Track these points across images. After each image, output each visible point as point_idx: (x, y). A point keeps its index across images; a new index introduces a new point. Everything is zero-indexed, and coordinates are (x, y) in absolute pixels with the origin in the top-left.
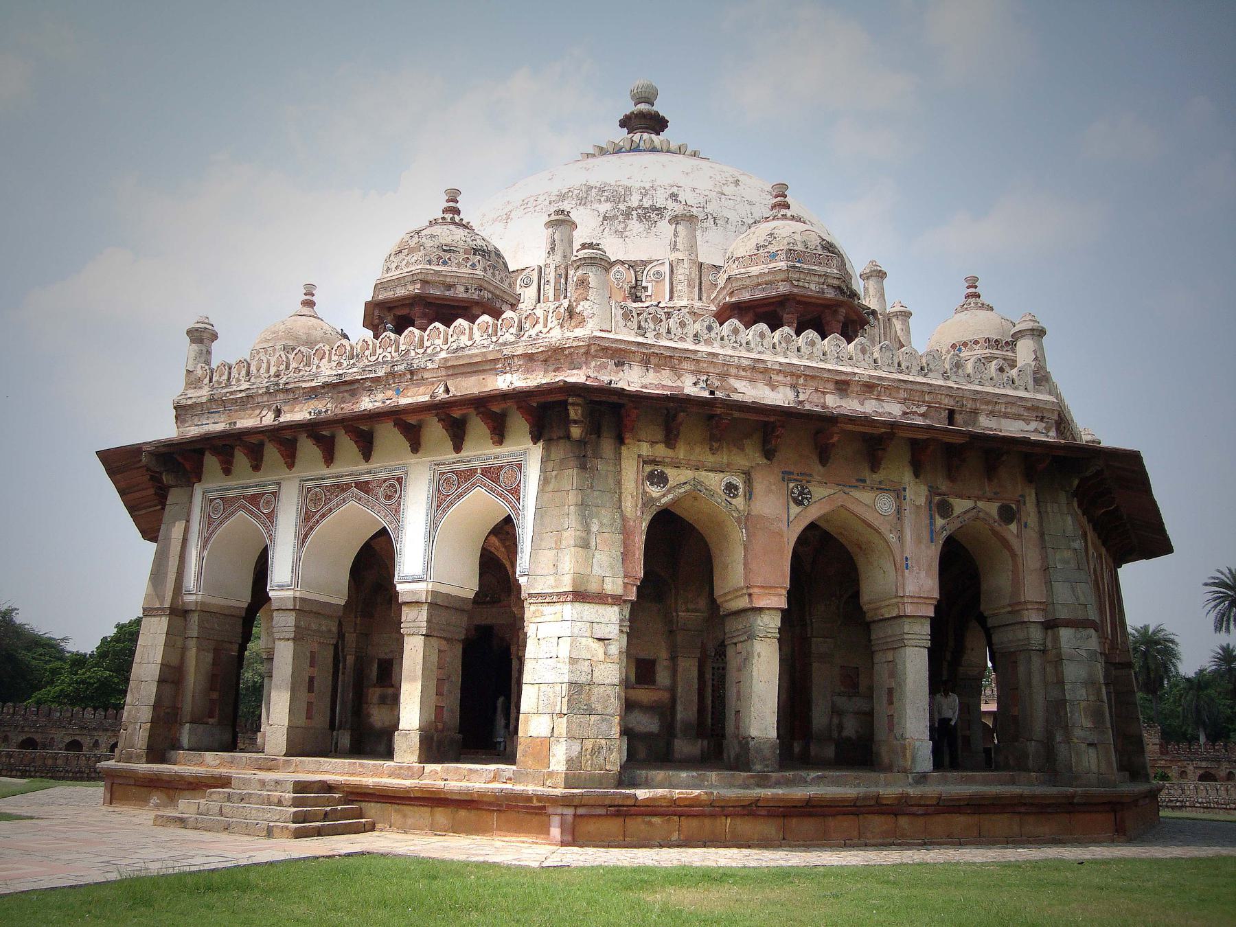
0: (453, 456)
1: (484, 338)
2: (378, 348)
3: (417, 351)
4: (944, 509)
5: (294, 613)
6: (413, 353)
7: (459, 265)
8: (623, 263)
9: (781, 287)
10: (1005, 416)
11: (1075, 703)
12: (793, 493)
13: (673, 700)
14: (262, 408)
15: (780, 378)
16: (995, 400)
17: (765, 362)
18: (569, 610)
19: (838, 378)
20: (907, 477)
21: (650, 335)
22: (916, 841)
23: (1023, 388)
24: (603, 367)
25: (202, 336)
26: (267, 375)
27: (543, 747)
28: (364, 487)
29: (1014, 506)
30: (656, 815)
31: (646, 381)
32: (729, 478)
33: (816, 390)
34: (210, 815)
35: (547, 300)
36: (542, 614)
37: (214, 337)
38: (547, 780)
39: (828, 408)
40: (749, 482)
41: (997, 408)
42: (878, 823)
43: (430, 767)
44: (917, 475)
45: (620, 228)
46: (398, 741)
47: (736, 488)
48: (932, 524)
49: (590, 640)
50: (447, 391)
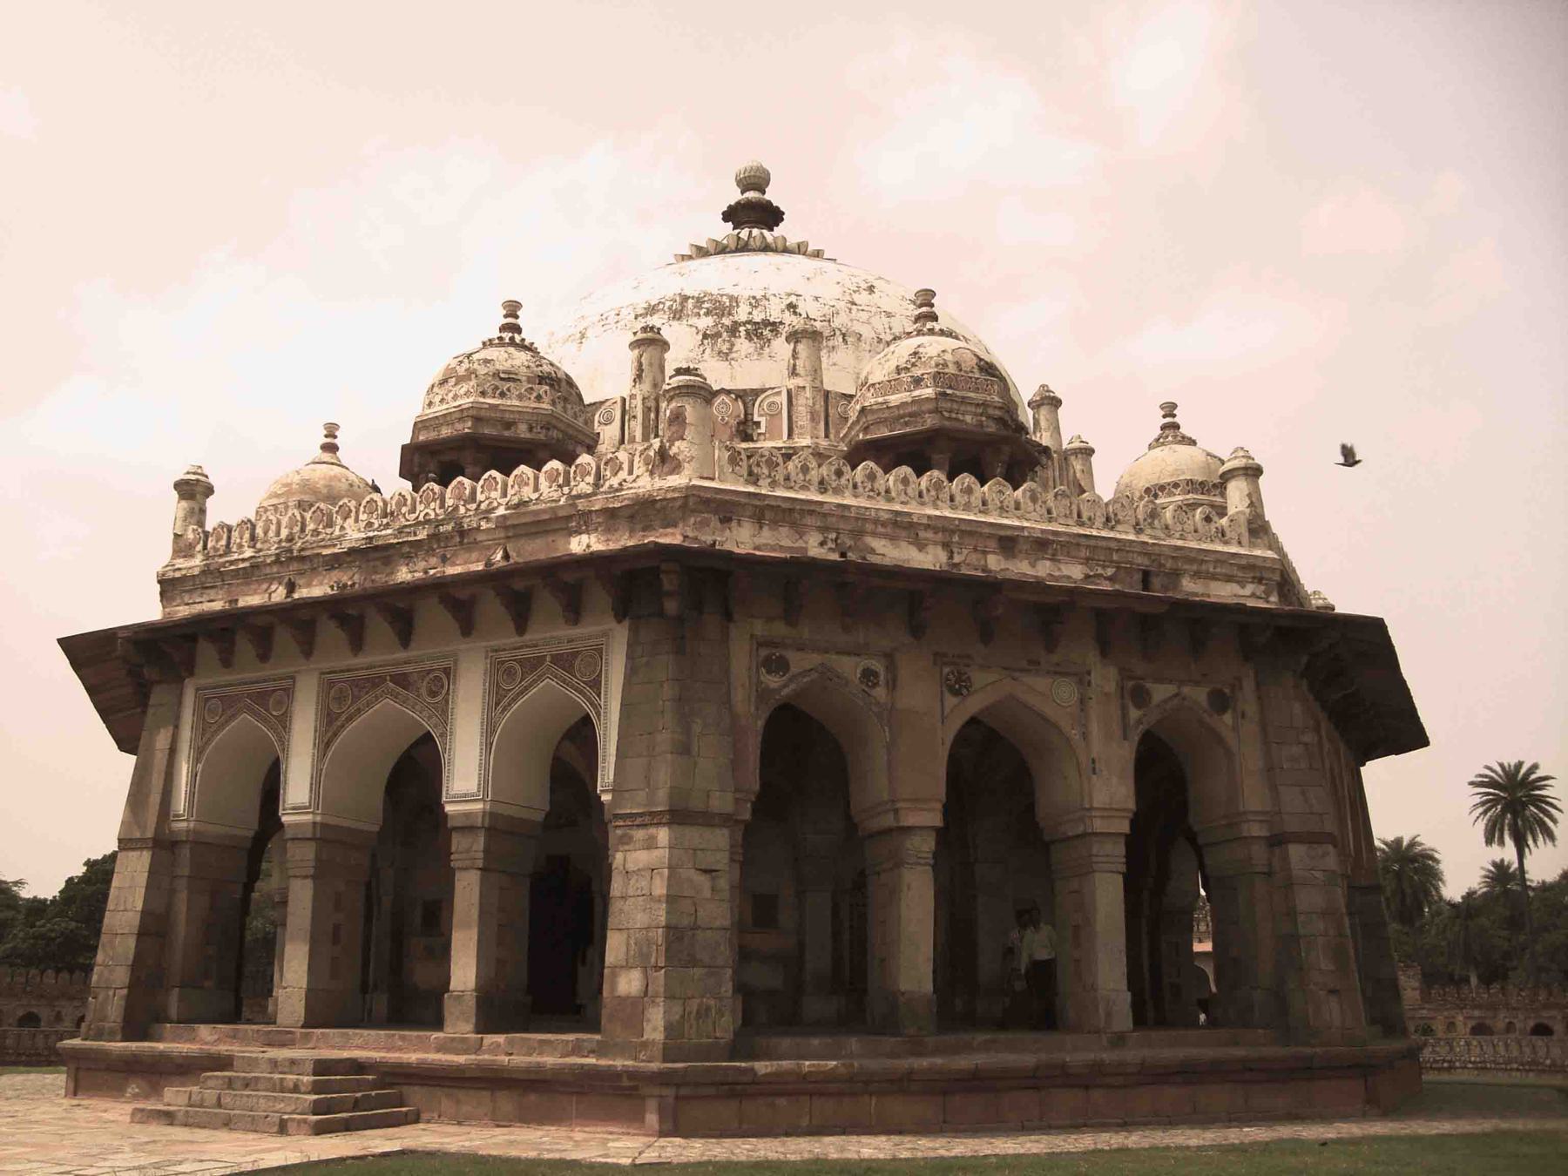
0: (515, 640)
1: (552, 489)
2: (418, 503)
3: (468, 506)
4: (1140, 696)
5: (313, 844)
6: (462, 510)
7: (520, 397)
8: (728, 392)
9: (929, 420)
10: (1214, 577)
13: (801, 946)
14: (271, 580)
15: (929, 535)
16: (1201, 557)
18: (663, 835)
19: (1002, 533)
20: (1092, 658)
23: (1235, 542)
24: (704, 524)
25: (194, 491)
26: (276, 539)
27: (635, 1009)
28: (402, 681)
29: (1227, 691)
31: (759, 541)
32: (865, 663)
34: (204, 1107)
35: (632, 440)
36: (631, 838)
37: (209, 490)
38: (640, 1052)
39: (990, 571)
40: (891, 667)
41: (1204, 567)
43: (490, 1039)
44: (1104, 653)
45: (725, 348)
46: (450, 1008)
47: (876, 674)
48: (1125, 716)
49: (693, 870)
50: (506, 556)
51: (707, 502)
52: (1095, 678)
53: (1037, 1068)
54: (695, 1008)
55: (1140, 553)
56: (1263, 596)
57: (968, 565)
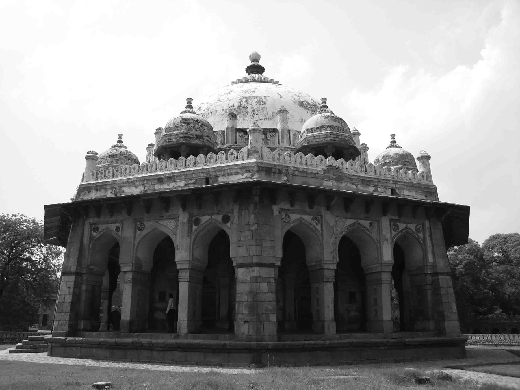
4: (197, 222)
11: (241, 302)
12: (138, 226)
15: (138, 183)
16: (223, 169)
17: (131, 179)
20: (180, 212)
21: (99, 179)
22: (158, 361)
24: (85, 194)
30: (74, 347)
31: (96, 196)
33: (152, 184)
39: (156, 190)
41: (226, 172)
42: (146, 353)
44: (184, 209)
51: (84, 188)
52: (181, 219)
53: (132, 343)
54: (61, 323)
55: (202, 173)
56: (250, 177)
57: (150, 189)
